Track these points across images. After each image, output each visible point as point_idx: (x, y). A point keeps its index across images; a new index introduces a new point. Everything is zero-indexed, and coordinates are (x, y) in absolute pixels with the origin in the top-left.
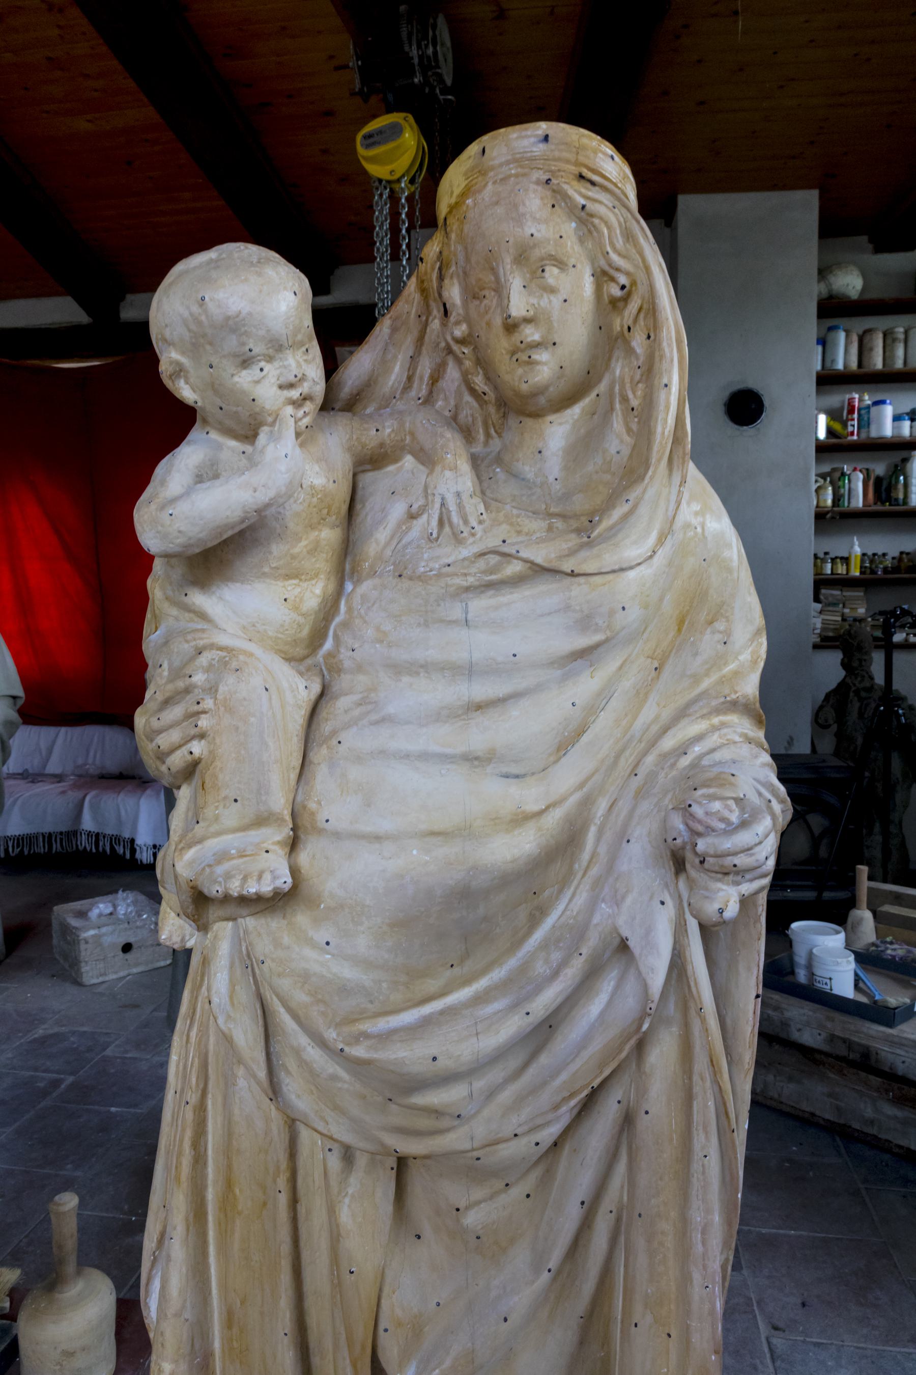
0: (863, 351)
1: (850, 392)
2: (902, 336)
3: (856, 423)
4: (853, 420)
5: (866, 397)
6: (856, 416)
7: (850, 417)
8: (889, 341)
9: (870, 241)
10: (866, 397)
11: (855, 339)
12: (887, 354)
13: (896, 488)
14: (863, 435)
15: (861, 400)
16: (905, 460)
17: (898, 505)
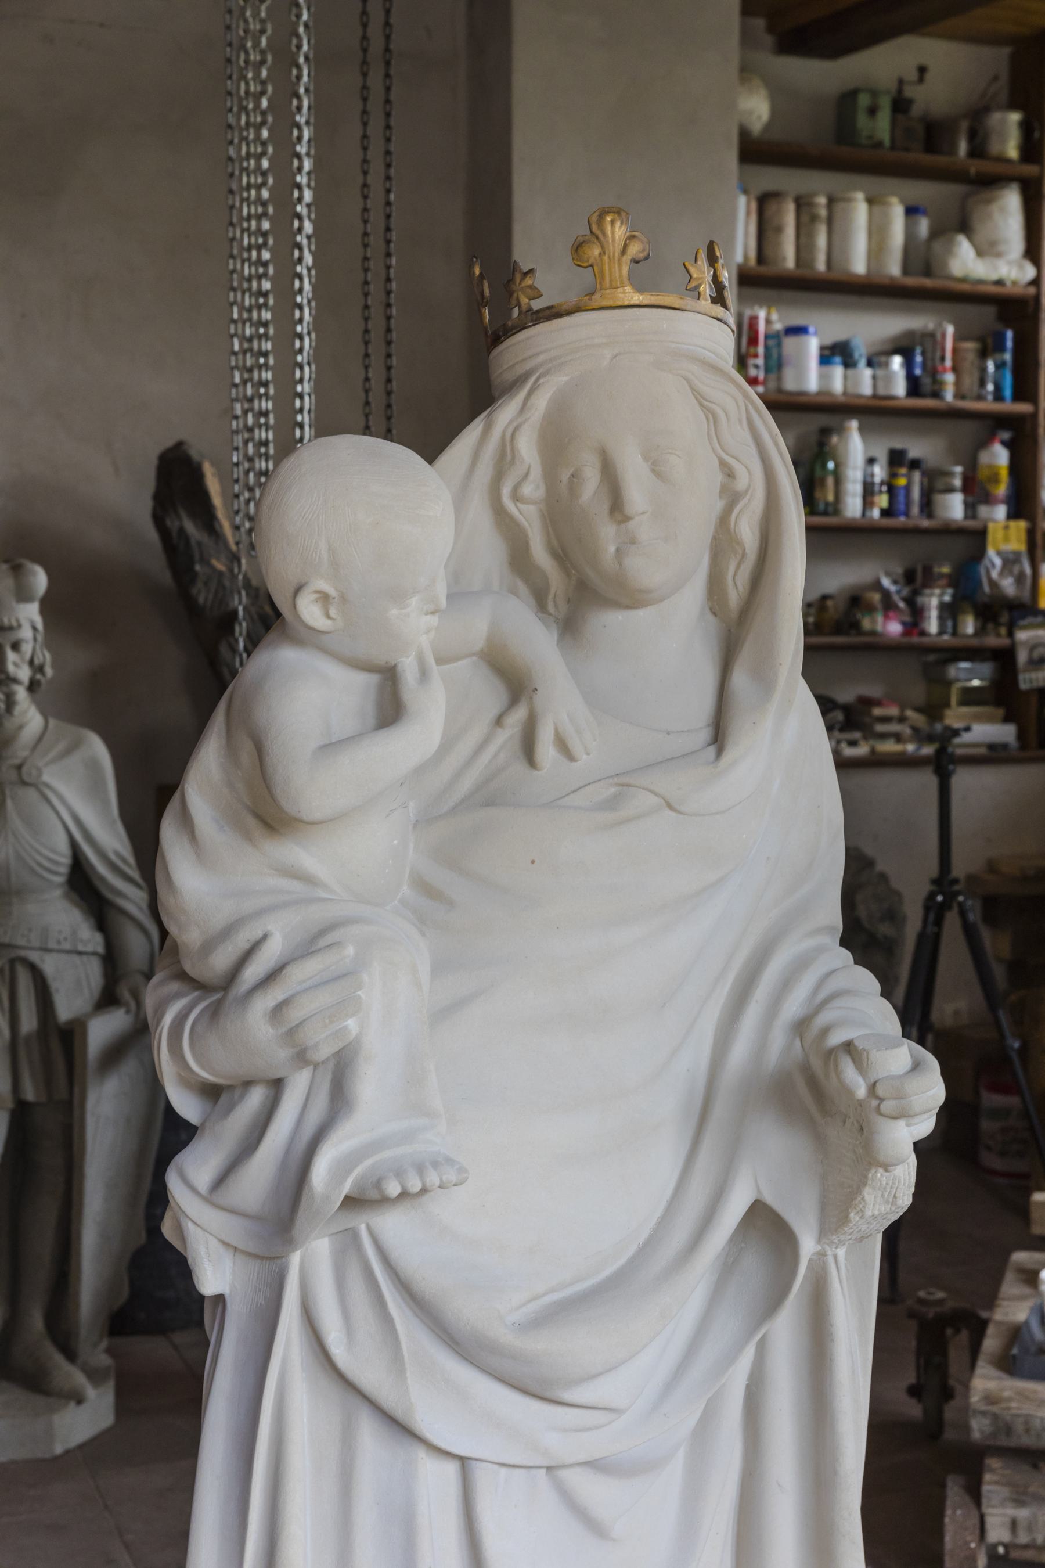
0: (766, 231)
1: (756, 308)
2: (823, 212)
3: (760, 361)
4: (756, 356)
5: (775, 316)
6: (761, 350)
7: (752, 350)
8: (805, 218)
9: (770, 29)
10: (775, 316)
11: (754, 206)
12: (803, 240)
13: (823, 482)
14: (772, 384)
15: (768, 322)
16: (825, 432)
17: (825, 513)
